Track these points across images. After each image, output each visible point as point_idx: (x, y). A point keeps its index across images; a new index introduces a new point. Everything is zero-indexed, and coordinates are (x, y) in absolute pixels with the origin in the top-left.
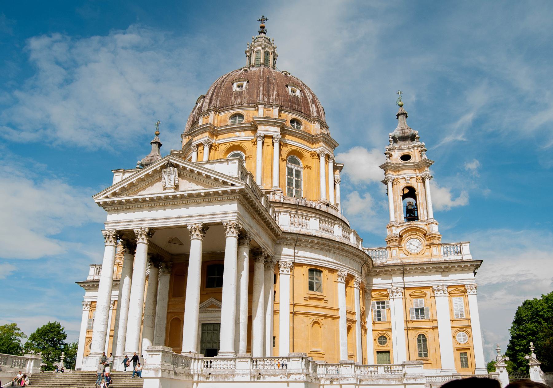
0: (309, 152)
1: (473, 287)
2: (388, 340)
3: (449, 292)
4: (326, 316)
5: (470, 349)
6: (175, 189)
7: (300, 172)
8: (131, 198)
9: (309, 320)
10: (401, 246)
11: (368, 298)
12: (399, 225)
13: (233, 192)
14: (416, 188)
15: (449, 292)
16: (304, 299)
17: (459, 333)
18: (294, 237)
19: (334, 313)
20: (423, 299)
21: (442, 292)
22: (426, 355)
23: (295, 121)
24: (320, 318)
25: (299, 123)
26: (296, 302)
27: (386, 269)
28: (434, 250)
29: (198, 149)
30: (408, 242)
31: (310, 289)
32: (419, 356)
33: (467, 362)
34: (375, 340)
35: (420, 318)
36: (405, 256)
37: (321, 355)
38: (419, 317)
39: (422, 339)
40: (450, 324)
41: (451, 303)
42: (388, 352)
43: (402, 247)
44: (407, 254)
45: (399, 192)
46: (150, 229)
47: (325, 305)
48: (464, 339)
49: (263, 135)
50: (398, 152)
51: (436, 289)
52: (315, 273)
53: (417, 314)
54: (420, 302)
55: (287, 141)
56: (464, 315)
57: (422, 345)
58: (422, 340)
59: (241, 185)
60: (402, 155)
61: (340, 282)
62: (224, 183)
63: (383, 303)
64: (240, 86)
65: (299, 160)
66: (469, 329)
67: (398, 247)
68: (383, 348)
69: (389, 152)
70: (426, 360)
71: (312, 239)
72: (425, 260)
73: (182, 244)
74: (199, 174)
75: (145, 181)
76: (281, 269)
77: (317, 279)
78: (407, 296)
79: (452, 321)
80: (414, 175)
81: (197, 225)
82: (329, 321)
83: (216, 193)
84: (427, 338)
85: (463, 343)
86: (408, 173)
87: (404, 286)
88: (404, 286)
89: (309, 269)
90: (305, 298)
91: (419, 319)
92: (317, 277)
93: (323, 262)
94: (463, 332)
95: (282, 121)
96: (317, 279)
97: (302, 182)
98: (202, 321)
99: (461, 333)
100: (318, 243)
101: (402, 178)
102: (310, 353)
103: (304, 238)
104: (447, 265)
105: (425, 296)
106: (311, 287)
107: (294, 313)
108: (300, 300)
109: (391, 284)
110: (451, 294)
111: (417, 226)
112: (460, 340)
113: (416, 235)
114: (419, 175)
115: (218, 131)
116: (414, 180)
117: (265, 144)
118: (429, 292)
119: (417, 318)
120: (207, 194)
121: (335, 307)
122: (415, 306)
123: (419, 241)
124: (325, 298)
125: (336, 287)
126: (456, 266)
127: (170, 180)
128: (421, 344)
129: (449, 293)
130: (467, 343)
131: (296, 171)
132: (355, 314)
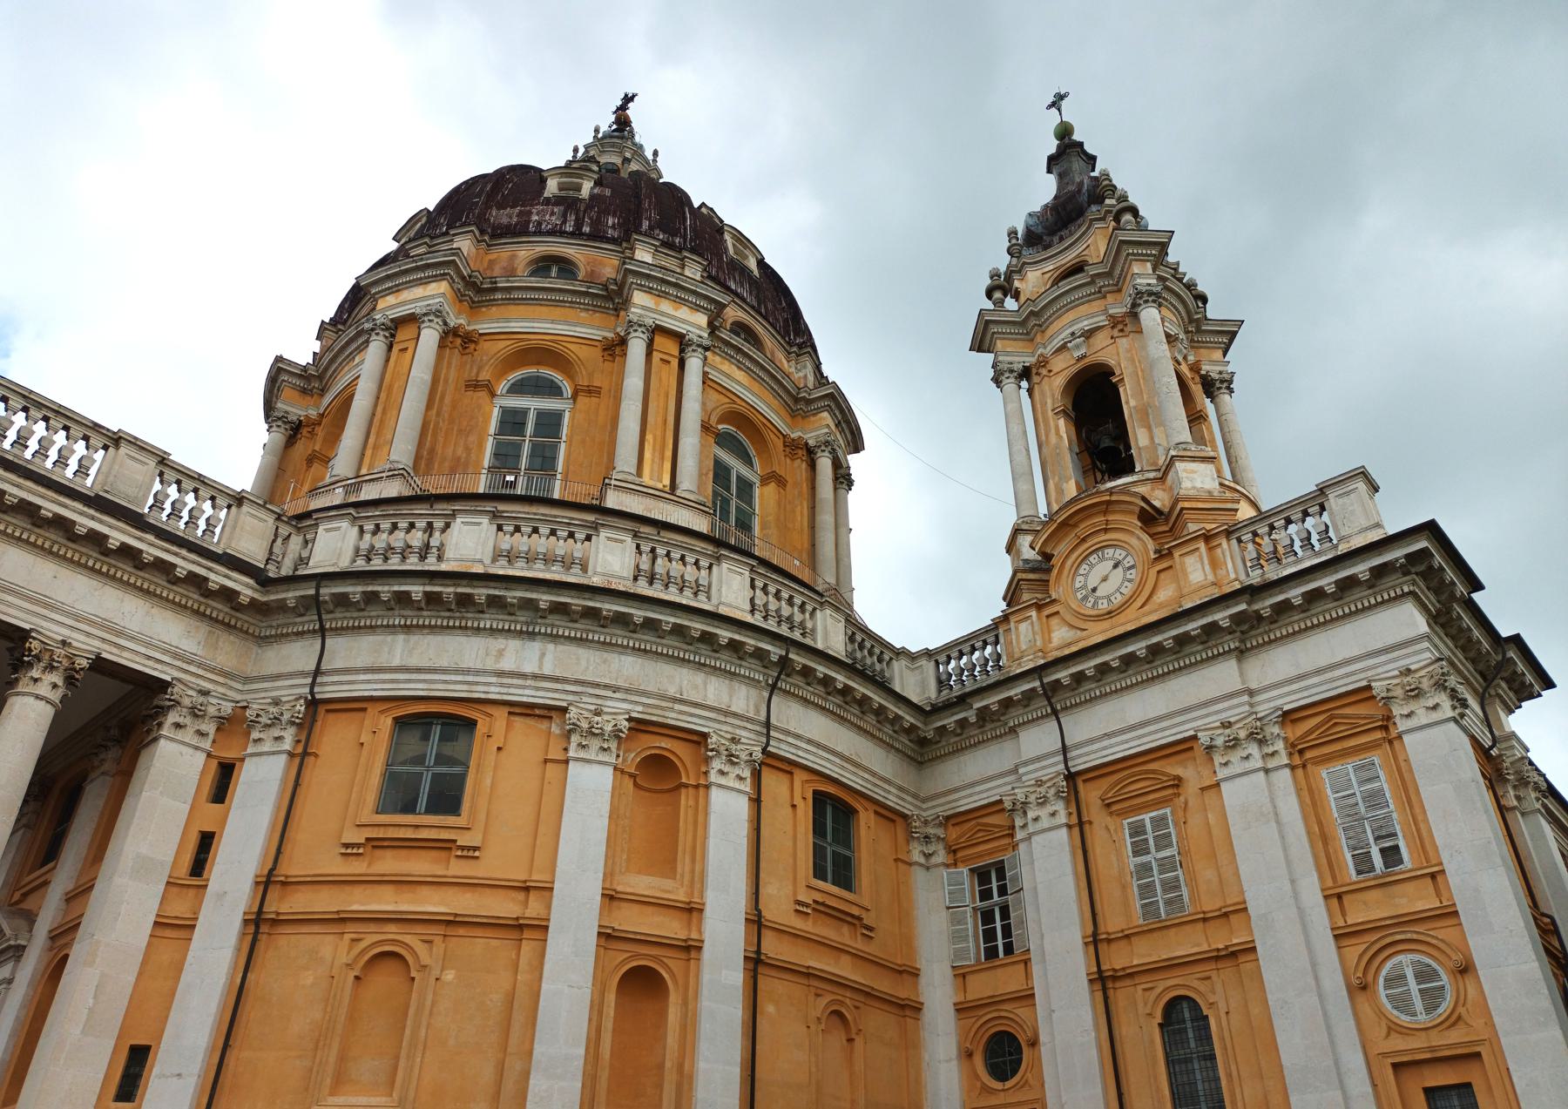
0: (597, 343)
1: (1426, 684)
2: (1026, 1053)
3: (1293, 745)
4: (452, 922)
5: (1478, 1055)
9: (335, 950)
14: (1112, 363)
15: (1293, 745)
16: (343, 851)
17: (1389, 965)
20: (1168, 811)
21: (1253, 749)
24: (411, 939)
26: (293, 867)
28: (1189, 570)
30: (1081, 571)
43: (1054, 601)
48: (1432, 998)
50: (1040, 272)
51: (1219, 742)
52: (436, 731)
60: (1055, 275)
66: (1442, 932)
67: (1039, 607)
71: (396, 588)
77: (441, 759)
78: (1094, 812)
79: (1339, 896)
80: (1101, 320)
82: (479, 946)
85: (1423, 1018)
89: (397, 720)
90: (346, 846)
92: (448, 749)
93: (470, 678)
94: (1417, 957)
95: (445, 256)
99: (1405, 962)
100: (432, 600)
104: (1243, 607)
105: (1170, 791)
109: (1015, 770)
110: (1308, 755)
112: (1402, 1003)
113: (1106, 530)
116: (1101, 339)
117: (395, 349)
118: (1191, 773)
122: (1136, 853)
123: (1124, 553)
129: (1296, 749)
130: (1454, 1021)
131: (541, 414)
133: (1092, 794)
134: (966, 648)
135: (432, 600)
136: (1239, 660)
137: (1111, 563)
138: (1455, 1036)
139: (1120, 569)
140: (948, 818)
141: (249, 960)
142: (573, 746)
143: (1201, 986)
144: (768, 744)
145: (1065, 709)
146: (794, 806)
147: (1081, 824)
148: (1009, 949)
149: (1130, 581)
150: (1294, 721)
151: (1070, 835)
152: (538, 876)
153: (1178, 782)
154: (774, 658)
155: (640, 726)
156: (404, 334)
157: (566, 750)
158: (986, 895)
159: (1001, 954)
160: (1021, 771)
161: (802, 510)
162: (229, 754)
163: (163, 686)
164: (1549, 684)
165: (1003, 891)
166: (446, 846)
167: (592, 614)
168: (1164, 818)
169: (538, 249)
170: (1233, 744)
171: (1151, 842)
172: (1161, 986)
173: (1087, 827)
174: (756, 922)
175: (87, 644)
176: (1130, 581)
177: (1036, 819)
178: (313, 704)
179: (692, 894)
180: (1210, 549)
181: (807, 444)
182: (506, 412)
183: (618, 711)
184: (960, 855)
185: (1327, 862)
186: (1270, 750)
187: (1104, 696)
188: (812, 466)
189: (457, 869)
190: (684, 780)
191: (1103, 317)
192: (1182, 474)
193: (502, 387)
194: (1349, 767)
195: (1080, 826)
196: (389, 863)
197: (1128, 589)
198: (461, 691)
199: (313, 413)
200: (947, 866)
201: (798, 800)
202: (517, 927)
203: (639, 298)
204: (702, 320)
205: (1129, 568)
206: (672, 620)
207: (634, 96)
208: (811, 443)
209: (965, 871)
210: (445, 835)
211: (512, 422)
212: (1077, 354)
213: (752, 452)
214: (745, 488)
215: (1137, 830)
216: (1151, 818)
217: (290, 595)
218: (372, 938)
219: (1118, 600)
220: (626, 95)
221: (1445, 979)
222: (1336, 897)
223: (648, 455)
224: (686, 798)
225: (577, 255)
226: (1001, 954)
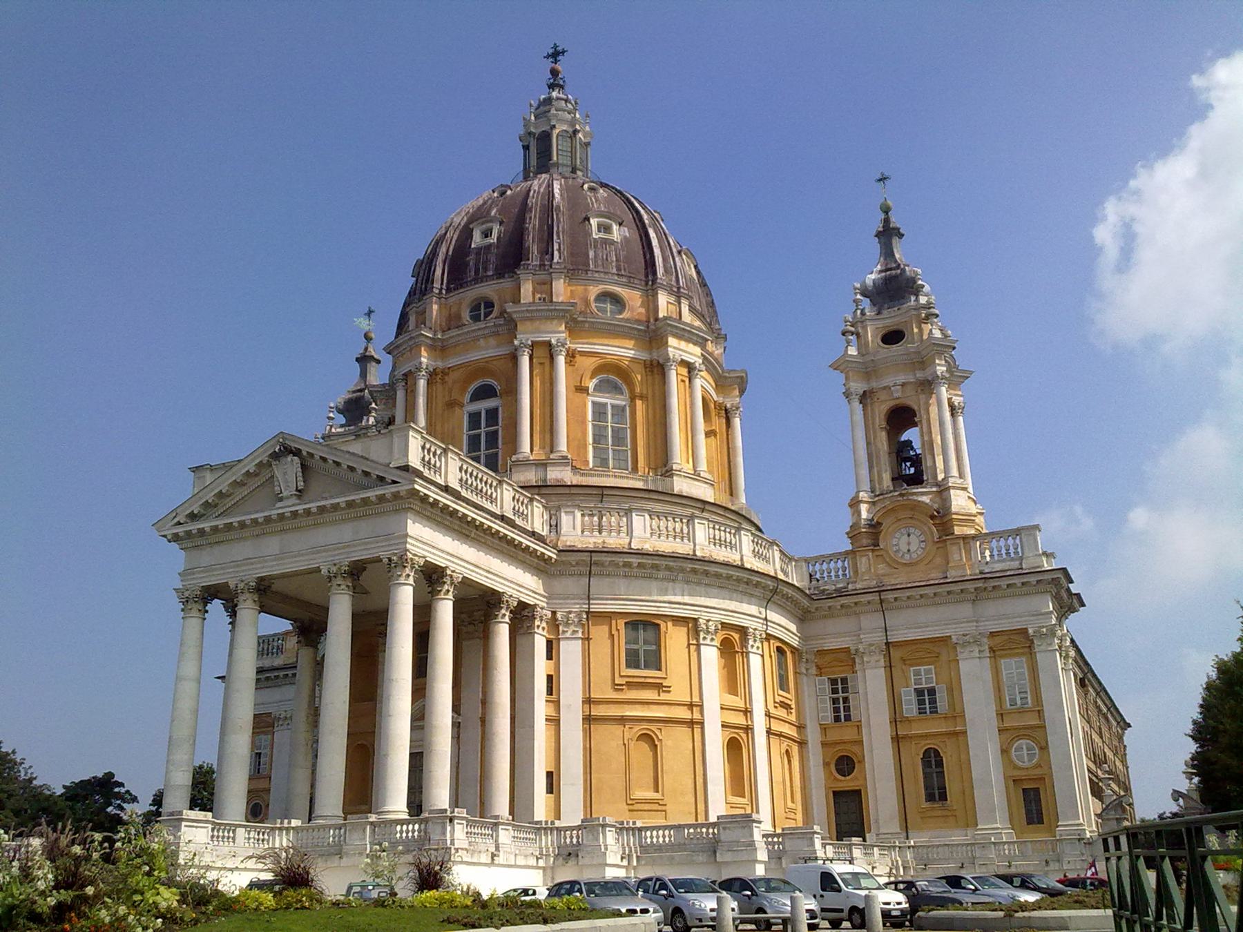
6: (299, 497)
8: (220, 522)
10: (878, 545)
11: (810, 671)
12: (877, 499)
13: (396, 496)
14: (916, 408)
15: (991, 648)
18: (585, 557)
20: (933, 667)
22: (943, 797)
27: (844, 601)
29: (406, 384)
31: (628, 666)
33: (1040, 813)
34: (826, 764)
35: (928, 712)
36: (887, 570)
38: (925, 708)
39: (933, 761)
40: (995, 723)
41: (996, 672)
42: (858, 793)
44: (894, 564)
45: (877, 419)
46: (261, 579)
47: (664, 697)
48: (1031, 757)
52: (641, 627)
53: (921, 702)
54: (926, 675)
56: (1029, 698)
57: (935, 775)
58: (933, 763)
59: (408, 482)
62: (381, 479)
63: (844, 681)
64: (487, 234)
68: (846, 783)
69: (853, 329)
71: (626, 560)
72: (935, 576)
73: (366, 593)
74: (338, 464)
75: (244, 485)
76: (561, 628)
79: (1002, 714)
81: (338, 566)
83: (365, 501)
84: (944, 759)
85: (1027, 764)
87: (887, 639)
88: (887, 639)
89: (626, 623)
91: (926, 713)
94: (1028, 741)
97: (628, 430)
101: (884, 388)
102: (629, 802)
103: (608, 558)
106: (633, 660)
107: (588, 720)
108: (603, 691)
112: (1020, 758)
113: (911, 518)
114: (920, 375)
115: (442, 340)
119: (922, 711)
120: (350, 505)
126: (1003, 583)
127: (286, 481)
128: (931, 774)
129: (992, 650)
130: (1039, 766)
134: (828, 560)
136: (973, 603)
138: (1038, 772)
141: (588, 734)
142: (702, 637)
144: (767, 629)
145: (887, 609)
147: (891, 667)
148: (848, 718)
149: (922, 548)
150: (993, 636)
151: (885, 671)
152: (696, 699)
155: (725, 626)
157: (698, 640)
158: (835, 691)
159: (843, 720)
160: (862, 636)
164: (1083, 605)
165: (845, 690)
166: (659, 687)
167: (706, 573)
168: (931, 669)
169: (601, 287)
170: (966, 644)
171: (924, 679)
172: (923, 743)
173: (893, 669)
174: (768, 715)
176: (922, 548)
178: (588, 613)
179: (746, 704)
181: (725, 407)
182: (594, 403)
183: (716, 617)
184: (823, 671)
186: (982, 649)
187: (908, 607)
189: (664, 697)
190: (737, 649)
191: (911, 377)
192: (952, 497)
193: (591, 390)
194: (1013, 662)
195: (890, 667)
198: (653, 611)
199: (440, 364)
200: (817, 675)
201: (773, 654)
202: (691, 723)
203: (672, 341)
205: (922, 542)
206: (737, 574)
207: (563, 52)
208: (728, 406)
210: (658, 681)
211: (599, 411)
212: (896, 395)
215: (917, 673)
216: (925, 670)
217: (572, 558)
218: (639, 729)
220: (555, 46)
221: (1037, 751)
222: (1001, 716)
224: (739, 658)
225: (623, 293)
226: (843, 720)
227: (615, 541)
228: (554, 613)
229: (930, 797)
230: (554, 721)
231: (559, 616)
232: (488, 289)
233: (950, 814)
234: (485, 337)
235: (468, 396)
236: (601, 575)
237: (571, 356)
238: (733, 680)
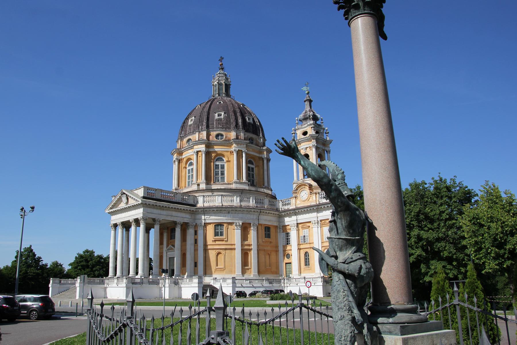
4: (226, 249)
7: (224, 165)
19: (233, 247)
20: (308, 230)
23: (220, 135)
24: (221, 251)
25: (222, 135)
32: (305, 266)
37: (222, 270)
39: (306, 254)
42: (291, 263)
49: (196, 151)
55: (215, 149)
61: (236, 229)
65: (223, 158)
70: (309, 268)
76: (198, 227)
77: (221, 230)
78: (300, 228)
80: (308, 146)
86: (304, 145)
96: (221, 230)
98: (169, 256)
100: (217, 210)
103: (208, 210)
104: (317, 207)
111: (305, 182)
121: (233, 243)
124: (225, 239)
125: (234, 232)
131: (221, 165)
132: (252, 245)
133: (300, 226)
135: (217, 210)
137: (305, 193)
139: (306, 194)
140: (283, 226)
143: (308, 251)
146: (262, 229)
153: (309, 227)
154: (259, 212)
156: (200, 153)
161: (262, 171)
162: (196, 229)
163: (188, 223)
166: (223, 240)
168: (307, 231)
175: (182, 222)
177: (293, 229)
180: (316, 195)
181: (262, 157)
185: (322, 239)
188: (263, 161)
195: (298, 230)
196: (217, 243)
197: (307, 197)
200: (282, 232)
201: (263, 229)
204: (245, 146)
208: (263, 157)
209: (285, 233)
213: (253, 161)
214: (253, 168)
219: (305, 199)
223: (239, 174)
227: (211, 204)
228: (196, 224)
229: (306, 265)
230: (196, 250)
231: (197, 225)
232: (190, 137)
233: (309, 269)
234: (189, 149)
235: (188, 165)
236: (208, 213)
237: (208, 154)
238: (244, 237)
